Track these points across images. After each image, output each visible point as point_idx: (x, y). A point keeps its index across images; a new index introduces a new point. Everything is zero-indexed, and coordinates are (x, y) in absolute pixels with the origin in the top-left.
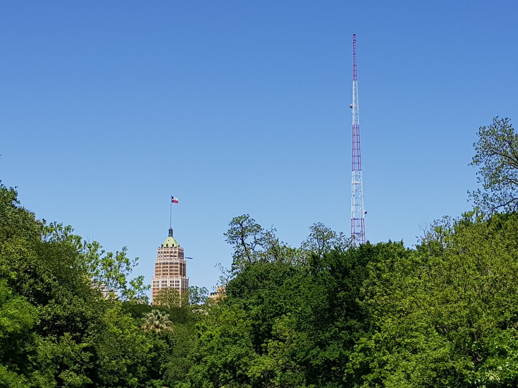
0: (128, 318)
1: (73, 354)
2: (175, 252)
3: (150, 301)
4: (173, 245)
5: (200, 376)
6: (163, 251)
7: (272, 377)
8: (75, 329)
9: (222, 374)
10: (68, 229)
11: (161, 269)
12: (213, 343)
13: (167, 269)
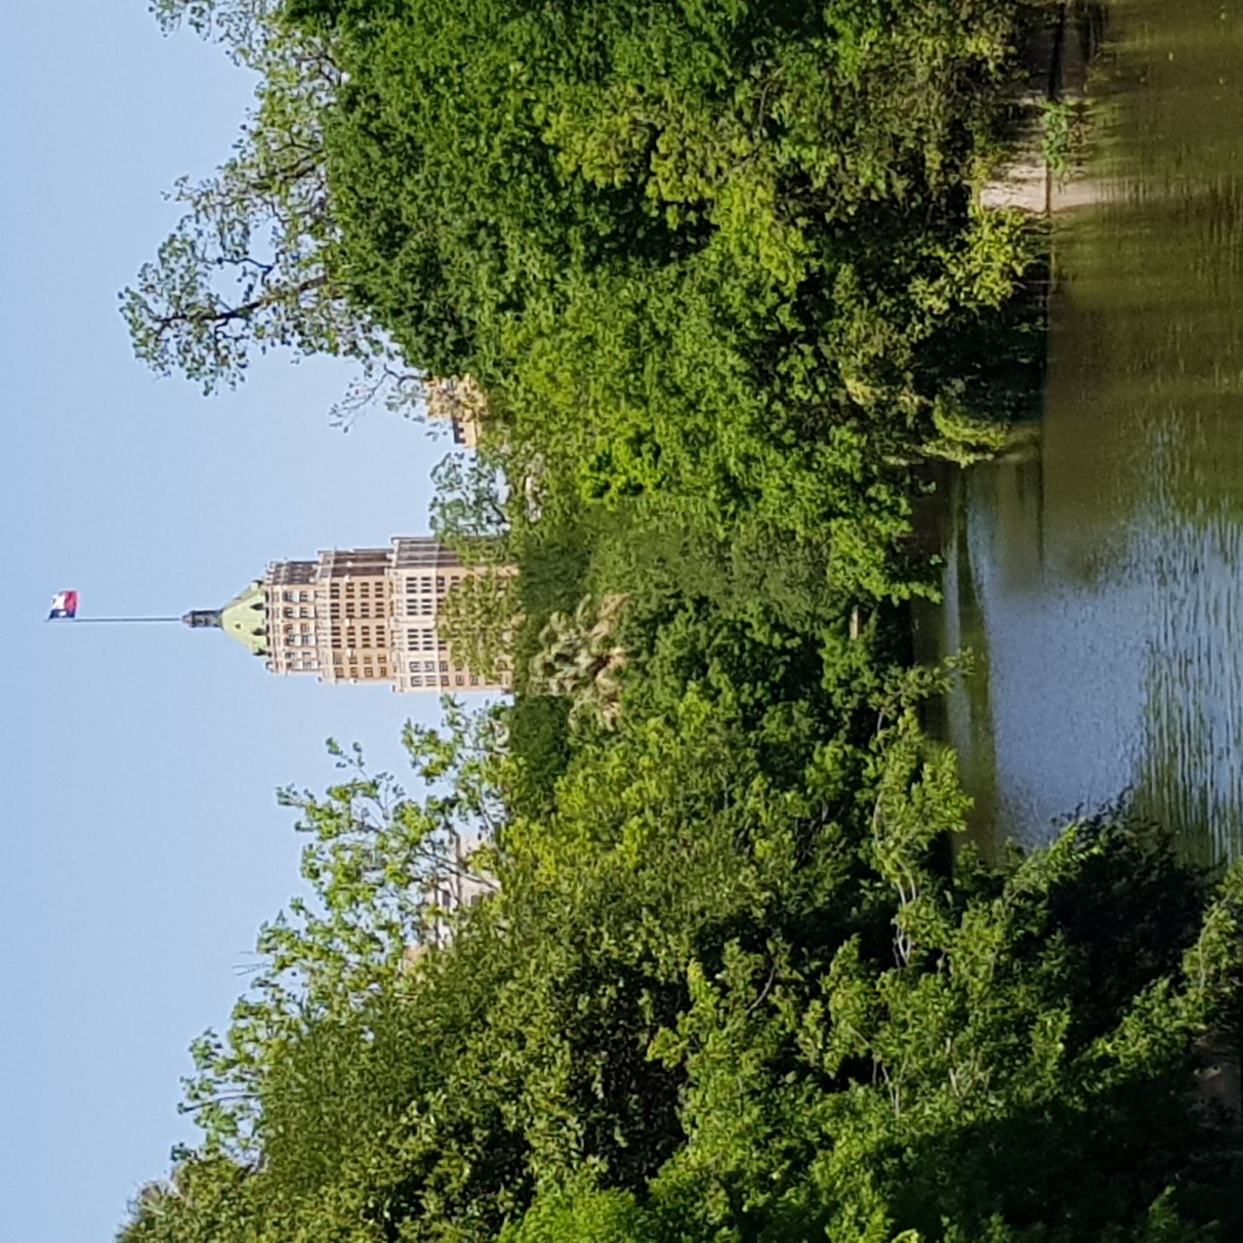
0: (574, 793)
1: (736, 1024)
2: (287, 597)
3: (499, 696)
4: (257, 607)
5: (806, 483)
6: (281, 648)
7: (803, 179)
8: (626, 1009)
9: (797, 391)
10: (206, 1055)
11: (360, 653)
12: (665, 432)
13: (358, 631)
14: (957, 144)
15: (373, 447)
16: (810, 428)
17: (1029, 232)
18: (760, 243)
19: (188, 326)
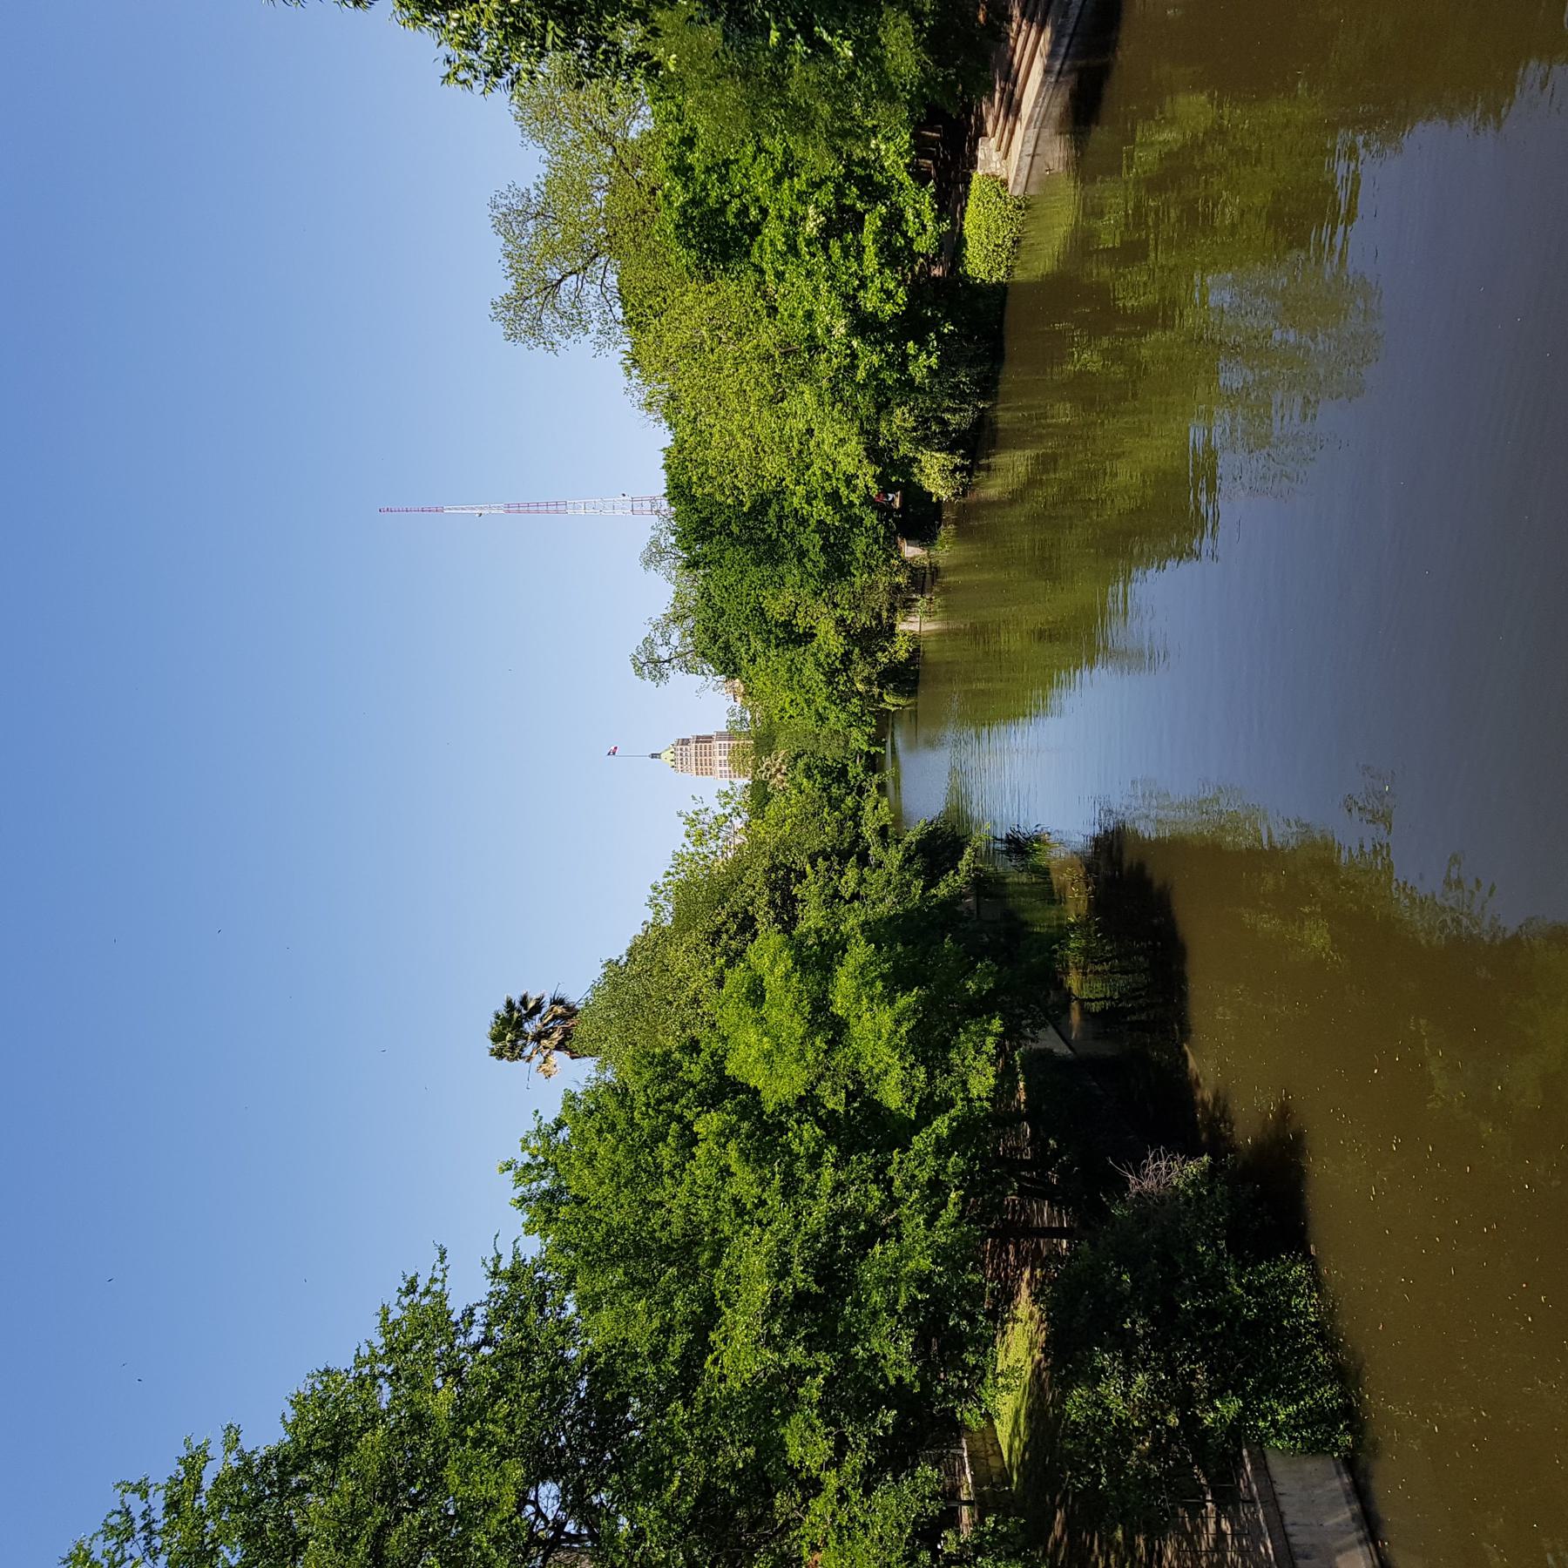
0: (771, 811)
3: (746, 781)
5: (843, 716)
7: (844, 621)
8: (787, 878)
9: (841, 687)
12: (800, 700)
14: (892, 609)
15: (709, 703)
16: (845, 699)
17: (914, 638)
18: (830, 640)
19: (651, 666)
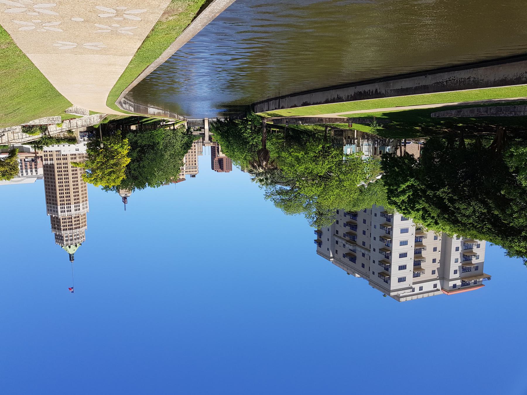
2: (67, 240)
4: (70, 247)
